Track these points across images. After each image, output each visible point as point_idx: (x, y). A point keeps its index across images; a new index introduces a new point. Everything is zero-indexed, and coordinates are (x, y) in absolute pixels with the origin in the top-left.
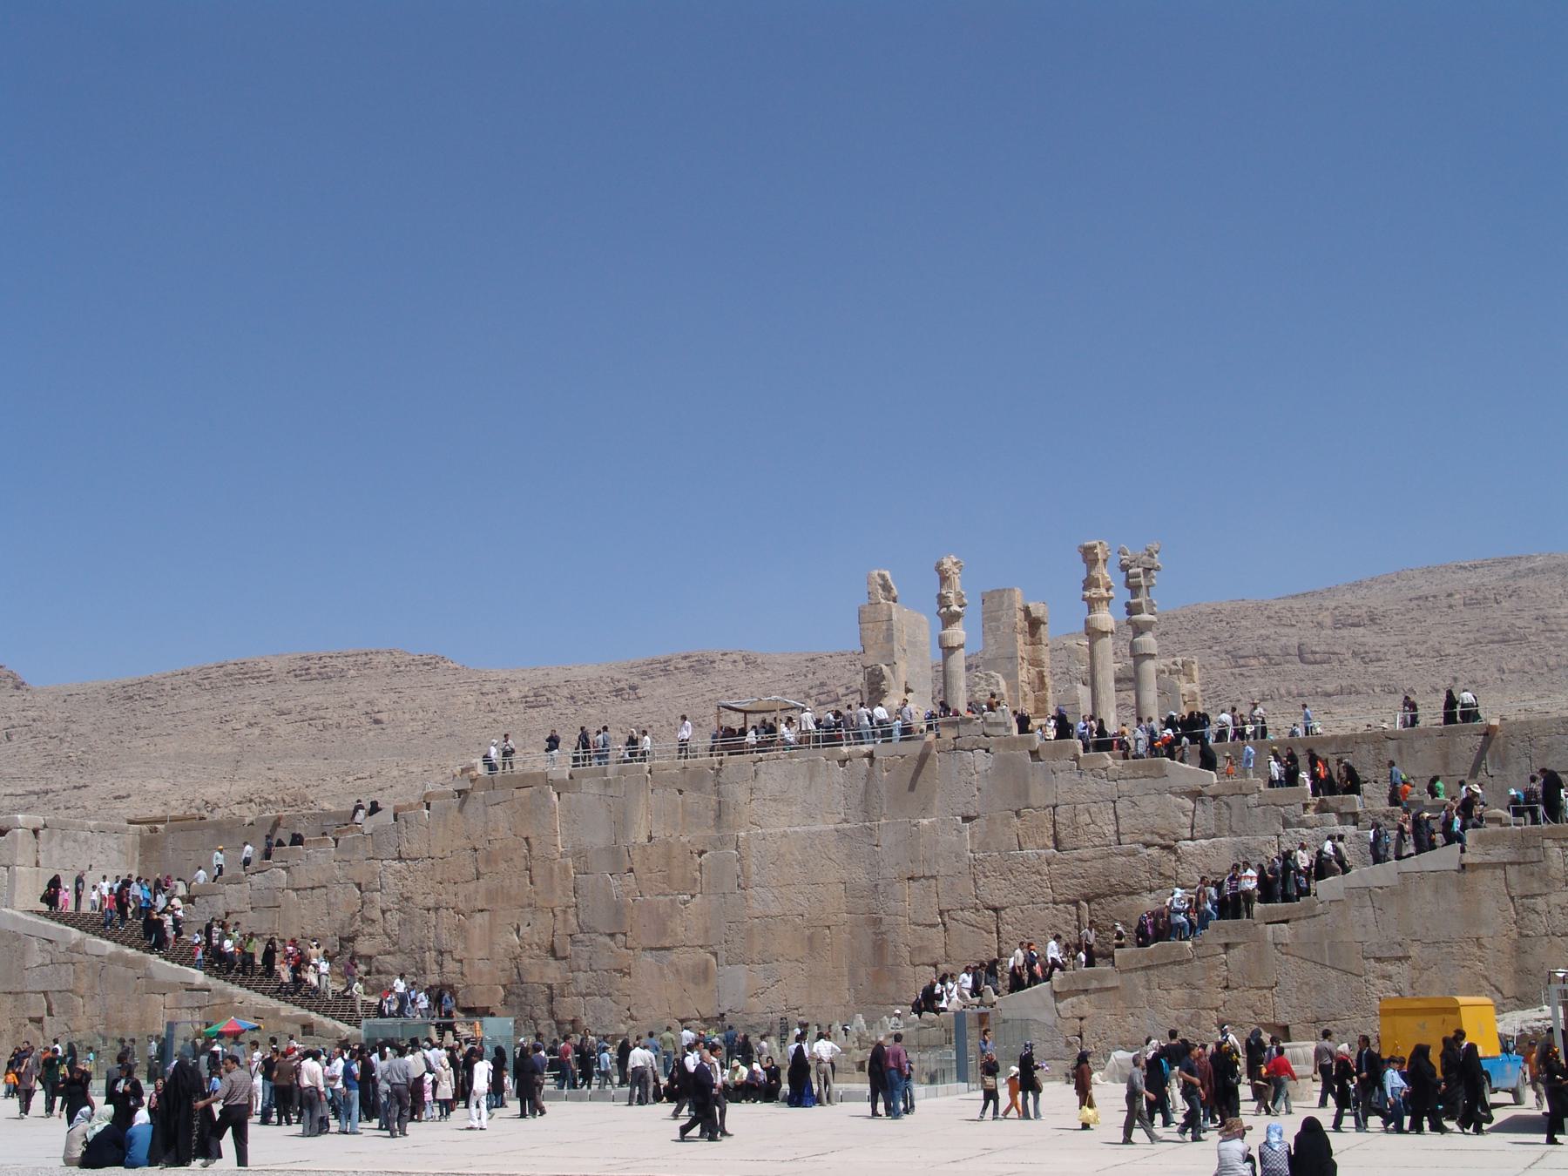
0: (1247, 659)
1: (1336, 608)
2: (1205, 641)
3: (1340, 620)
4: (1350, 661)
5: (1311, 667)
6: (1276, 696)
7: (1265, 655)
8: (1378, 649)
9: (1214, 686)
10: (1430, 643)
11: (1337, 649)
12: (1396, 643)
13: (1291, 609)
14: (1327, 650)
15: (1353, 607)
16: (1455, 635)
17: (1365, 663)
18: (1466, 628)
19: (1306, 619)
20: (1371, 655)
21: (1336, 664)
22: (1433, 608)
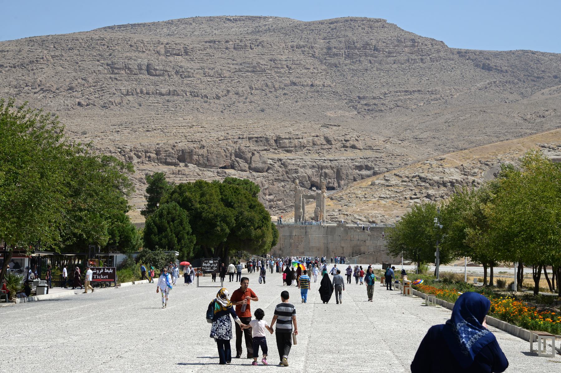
0: (119, 71)
1: (167, 44)
2: (95, 56)
3: (169, 51)
4: (174, 76)
5: (153, 78)
6: (135, 93)
7: (129, 69)
8: (189, 70)
9: (101, 84)
10: (216, 69)
11: (168, 69)
12: (199, 68)
13: (142, 42)
14: (162, 69)
15: (176, 44)
16: (229, 65)
17: (182, 78)
18: (235, 62)
19: (151, 49)
20: (185, 74)
21: (167, 77)
22: (218, 48)
